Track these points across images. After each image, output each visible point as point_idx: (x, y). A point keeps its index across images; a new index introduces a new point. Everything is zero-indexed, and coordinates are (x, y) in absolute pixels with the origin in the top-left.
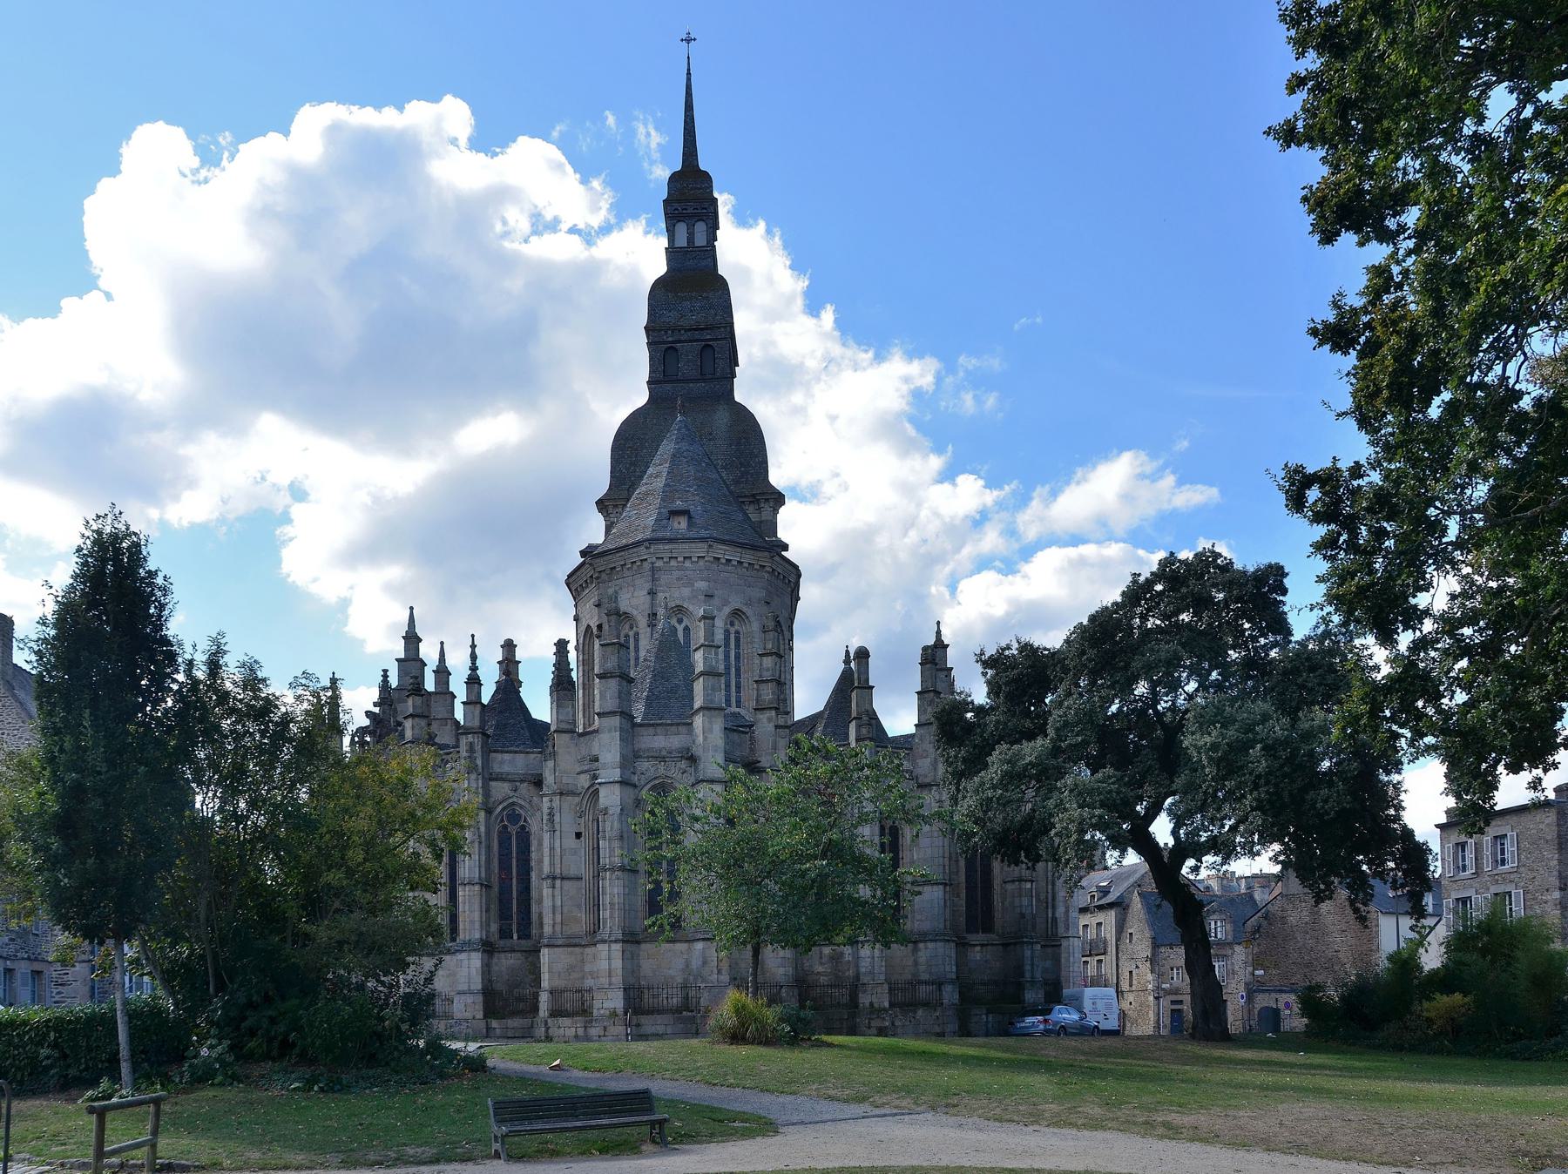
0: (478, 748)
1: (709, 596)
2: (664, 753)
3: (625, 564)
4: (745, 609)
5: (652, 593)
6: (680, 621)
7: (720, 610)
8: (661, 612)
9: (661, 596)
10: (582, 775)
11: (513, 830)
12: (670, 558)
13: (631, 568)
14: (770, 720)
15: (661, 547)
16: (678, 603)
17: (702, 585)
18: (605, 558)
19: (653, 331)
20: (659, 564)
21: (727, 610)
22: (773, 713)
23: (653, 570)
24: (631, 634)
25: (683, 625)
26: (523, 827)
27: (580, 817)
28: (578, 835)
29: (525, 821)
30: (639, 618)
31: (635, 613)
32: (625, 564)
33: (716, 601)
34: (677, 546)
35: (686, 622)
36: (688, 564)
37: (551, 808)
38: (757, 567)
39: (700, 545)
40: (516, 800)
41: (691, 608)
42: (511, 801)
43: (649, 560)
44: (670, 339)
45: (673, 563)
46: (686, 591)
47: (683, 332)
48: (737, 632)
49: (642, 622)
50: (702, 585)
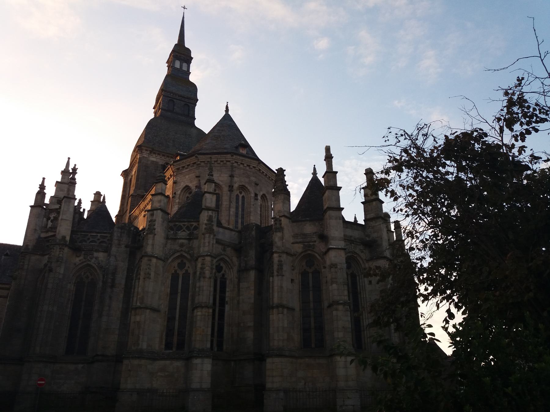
1: (257, 184)
2: (352, 239)
3: (217, 161)
4: (267, 195)
5: (232, 176)
6: (241, 193)
8: (236, 186)
9: (236, 179)
10: (296, 245)
11: (219, 275)
12: (241, 163)
13: (219, 163)
15: (238, 157)
16: (243, 184)
17: (253, 179)
18: (206, 156)
19: (165, 91)
20: (235, 164)
23: (232, 167)
25: (242, 195)
26: (223, 275)
27: (293, 270)
28: (292, 280)
29: (225, 271)
30: (223, 186)
31: (221, 183)
32: (217, 161)
33: (258, 187)
34: (245, 159)
35: (243, 194)
36: (248, 168)
37: (280, 261)
38: (271, 179)
39: (255, 162)
40: (224, 257)
41: (249, 188)
42: (222, 257)
43: (231, 162)
44: (172, 97)
45: (241, 166)
47: (177, 96)
49: (226, 189)
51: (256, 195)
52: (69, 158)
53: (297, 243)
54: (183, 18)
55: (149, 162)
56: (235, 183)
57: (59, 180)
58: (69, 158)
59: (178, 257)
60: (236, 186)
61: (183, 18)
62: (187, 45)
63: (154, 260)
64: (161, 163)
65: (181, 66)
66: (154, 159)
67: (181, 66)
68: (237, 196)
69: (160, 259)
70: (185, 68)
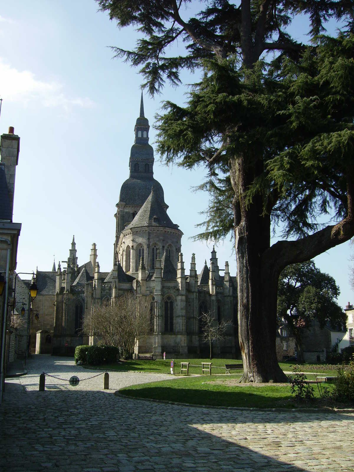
0: (117, 282)
1: (163, 241)
4: (172, 244)
7: (166, 244)
8: (151, 244)
10: (147, 291)
14: (193, 280)
17: (161, 238)
21: (168, 244)
22: (194, 278)
24: (141, 249)
45: (154, 231)
46: (157, 239)
48: (169, 250)
50: (161, 238)
51: (163, 247)
52: (74, 236)
53: (147, 291)
54: (142, 93)
55: (124, 213)
56: (151, 242)
57: (71, 249)
58: (74, 236)
59: (106, 297)
60: (151, 244)
61: (142, 93)
62: (146, 117)
63: (96, 300)
64: (131, 212)
65: (142, 135)
66: (127, 211)
67: (142, 135)
68: (153, 249)
69: (99, 299)
70: (145, 136)
